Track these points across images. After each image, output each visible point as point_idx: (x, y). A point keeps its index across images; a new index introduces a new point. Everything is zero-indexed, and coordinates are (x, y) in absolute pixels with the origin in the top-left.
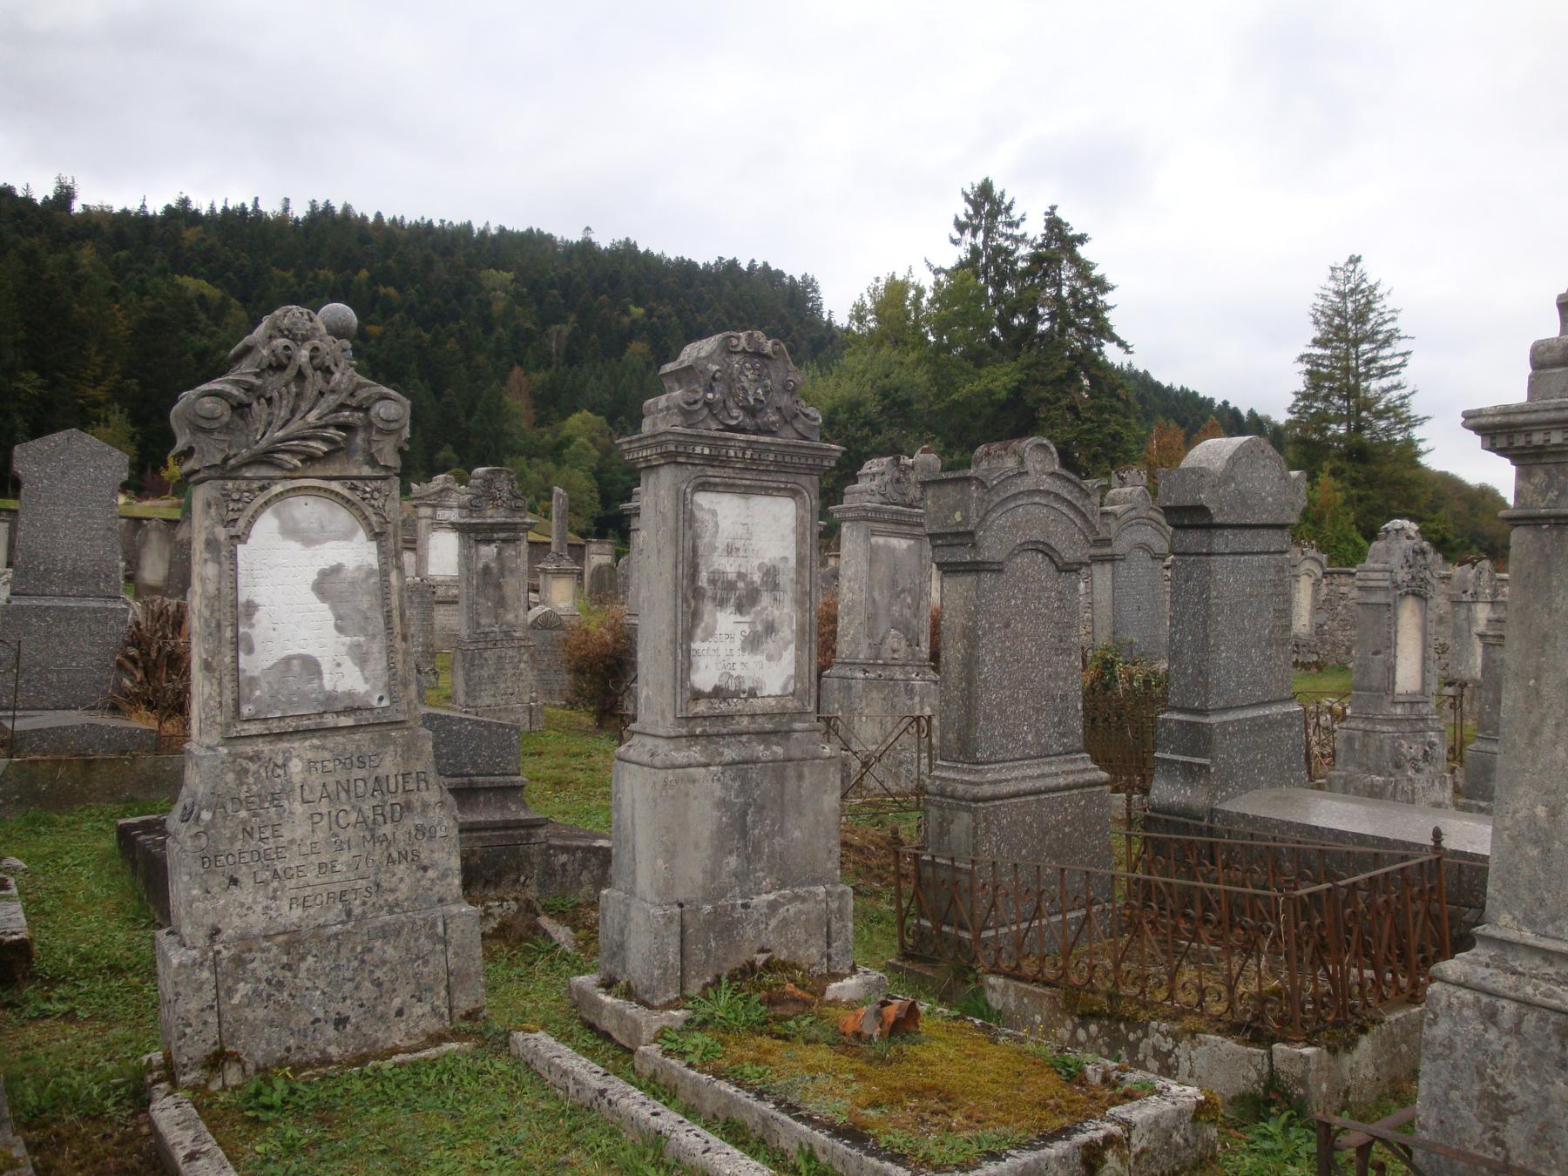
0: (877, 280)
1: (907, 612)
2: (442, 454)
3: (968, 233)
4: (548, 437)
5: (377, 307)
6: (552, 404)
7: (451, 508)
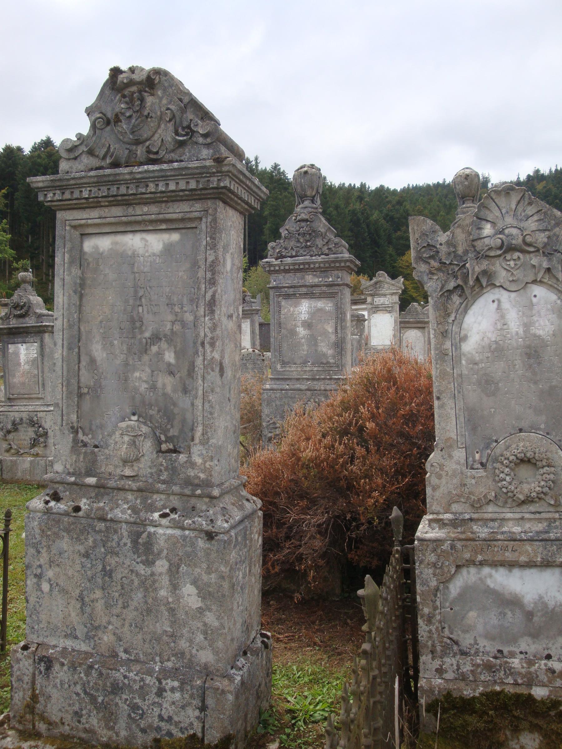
1: (167, 383)
7: (385, 295)
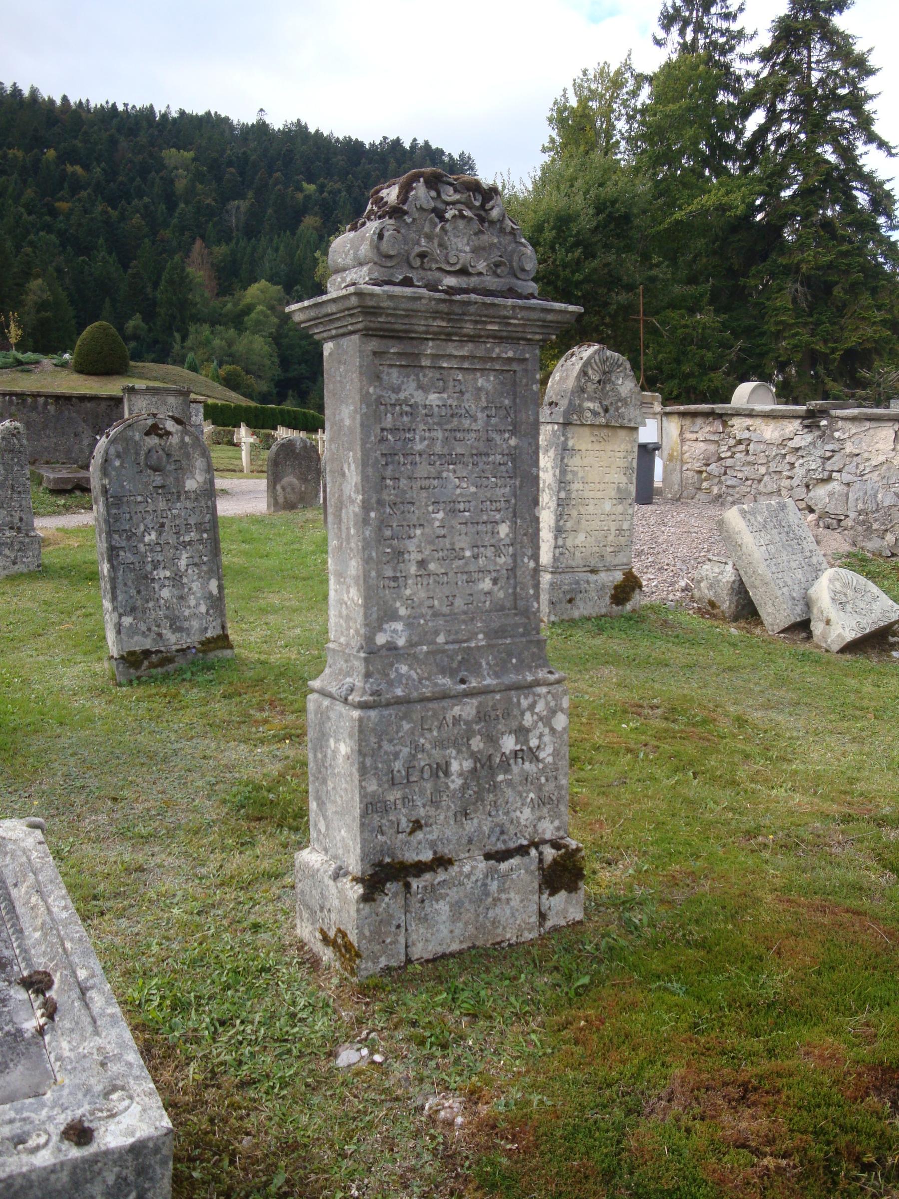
0: (585, 73)
2: (131, 323)
3: (675, 30)
4: (229, 306)
5: (66, 185)
6: (231, 276)
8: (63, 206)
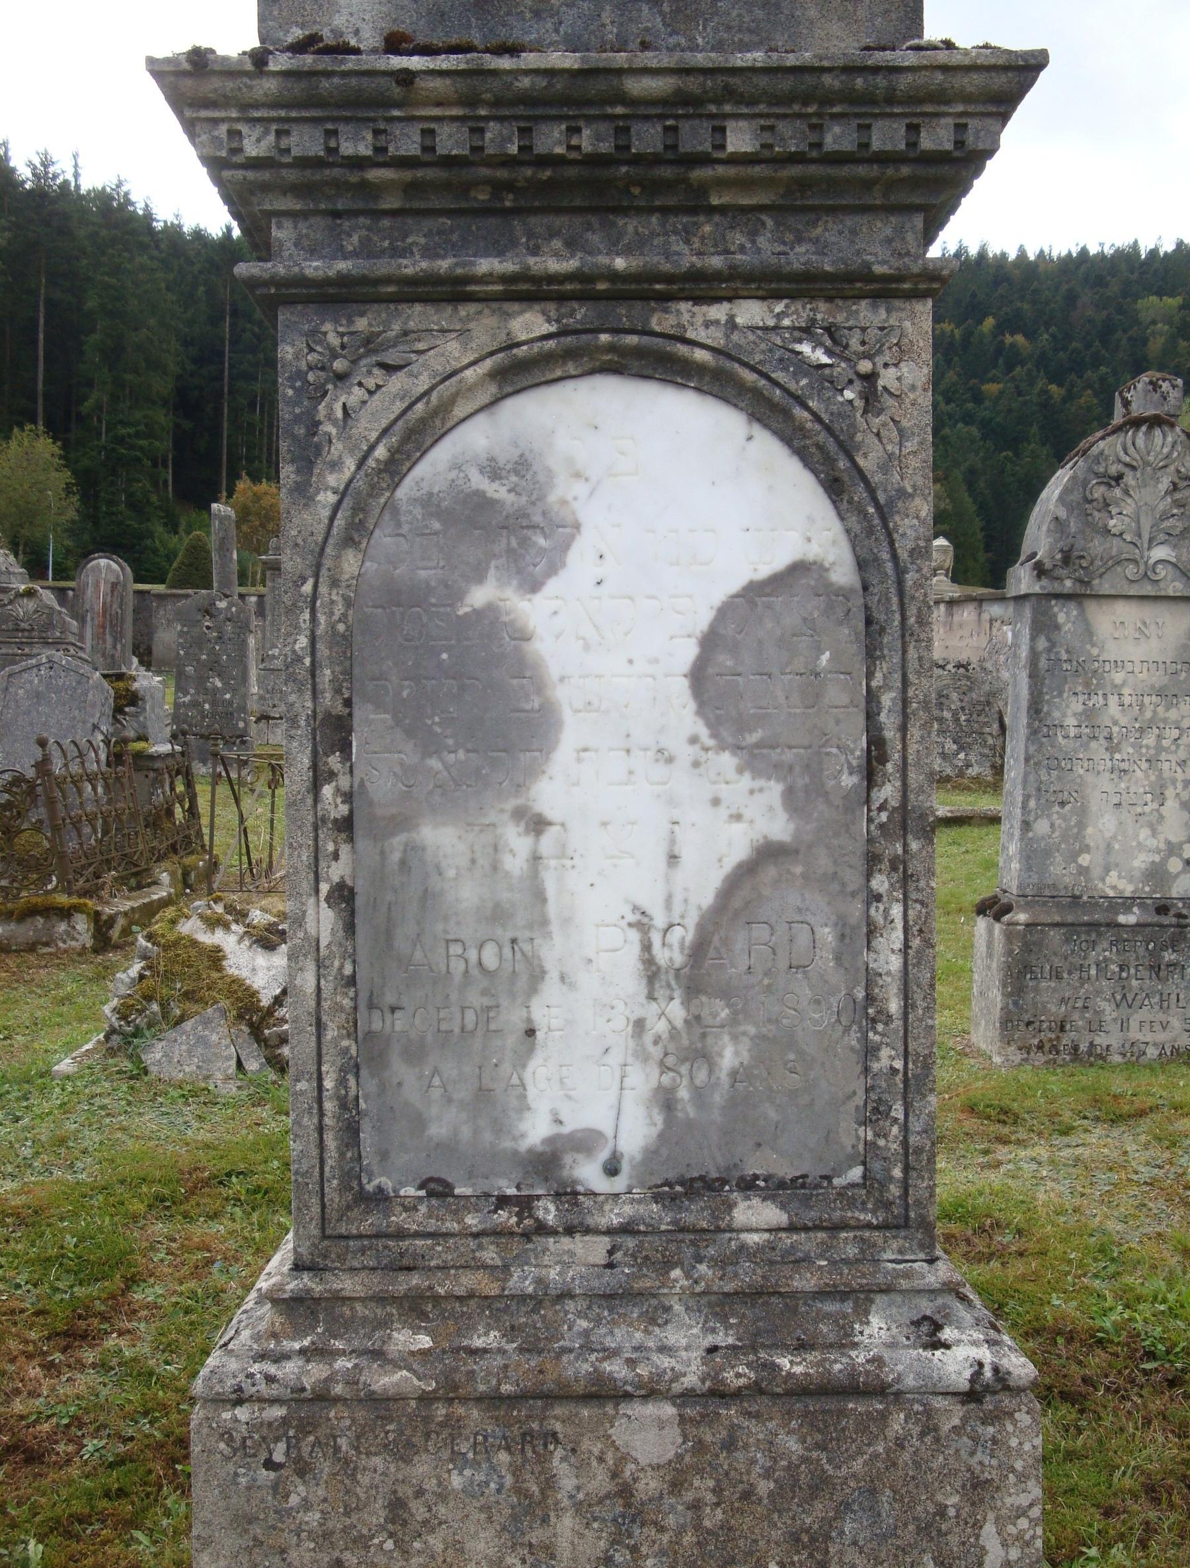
5: (1001, 361)
8: (991, 388)
